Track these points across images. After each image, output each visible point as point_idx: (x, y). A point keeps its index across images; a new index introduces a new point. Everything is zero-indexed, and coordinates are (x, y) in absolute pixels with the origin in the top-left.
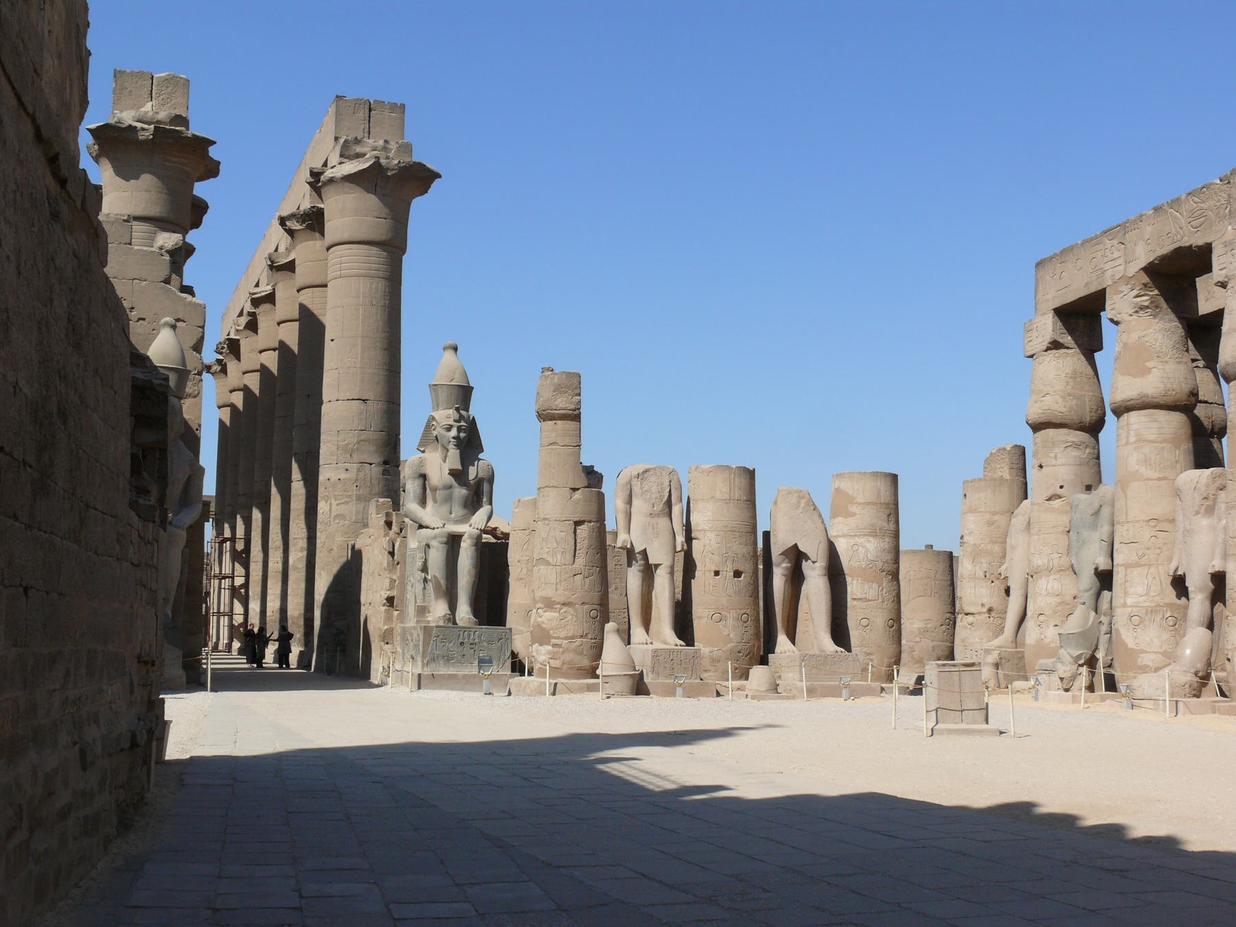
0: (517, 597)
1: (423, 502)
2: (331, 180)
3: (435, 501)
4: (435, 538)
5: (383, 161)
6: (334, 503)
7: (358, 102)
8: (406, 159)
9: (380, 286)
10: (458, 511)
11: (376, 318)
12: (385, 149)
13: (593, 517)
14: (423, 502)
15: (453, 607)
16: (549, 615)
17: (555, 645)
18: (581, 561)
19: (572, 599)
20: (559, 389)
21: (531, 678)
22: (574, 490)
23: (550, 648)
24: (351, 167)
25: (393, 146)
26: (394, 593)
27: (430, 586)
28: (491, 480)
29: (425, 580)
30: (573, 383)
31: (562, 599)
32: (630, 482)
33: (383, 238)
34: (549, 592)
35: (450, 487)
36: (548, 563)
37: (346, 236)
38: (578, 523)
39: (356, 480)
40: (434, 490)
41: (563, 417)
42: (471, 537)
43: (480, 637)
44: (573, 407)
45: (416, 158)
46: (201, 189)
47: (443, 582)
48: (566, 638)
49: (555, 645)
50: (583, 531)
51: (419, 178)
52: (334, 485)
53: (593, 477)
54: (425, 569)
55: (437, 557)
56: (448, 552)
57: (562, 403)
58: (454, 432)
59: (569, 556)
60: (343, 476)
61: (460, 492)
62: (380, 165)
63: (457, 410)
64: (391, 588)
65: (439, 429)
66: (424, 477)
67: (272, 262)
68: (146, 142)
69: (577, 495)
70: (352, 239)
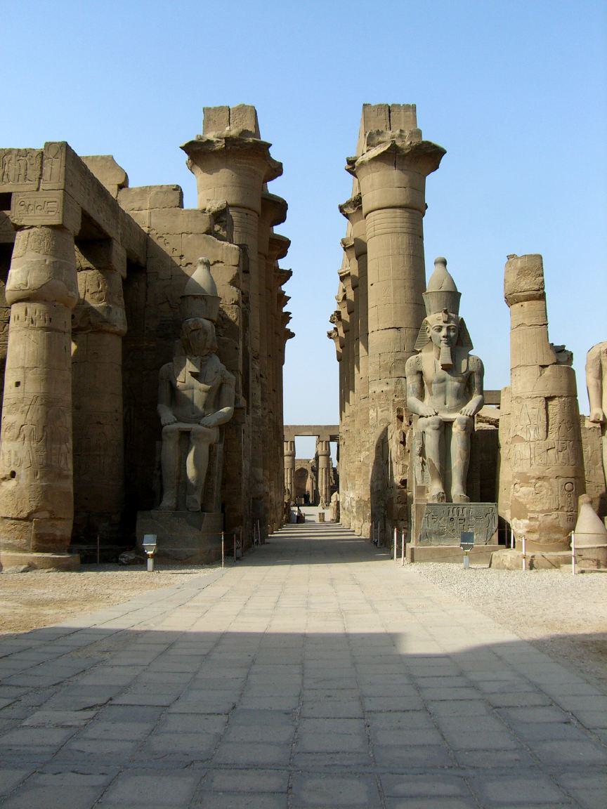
0: (506, 473)
1: (421, 396)
2: (362, 164)
3: (431, 394)
4: (428, 425)
5: (399, 144)
6: (379, 410)
7: (380, 107)
8: (416, 141)
9: (404, 239)
10: (451, 401)
11: (403, 263)
12: (401, 136)
13: (564, 393)
14: (421, 396)
15: (447, 486)
16: (524, 489)
17: (531, 519)
18: (553, 436)
19: (547, 473)
20: (522, 272)
21: (514, 550)
22: (543, 367)
23: (527, 521)
24: (376, 152)
25: (407, 134)
26: (406, 477)
27: (427, 468)
28: (481, 372)
29: (423, 463)
30: (534, 265)
31: (537, 474)
32: (599, 357)
33: (404, 203)
34: (524, 468)
35: (444, 380)
36: (522, 440)
37: (376, 205)
38: (548, 399)
39: (395, 391)
40: (430, 384)
41: (530, 298)
42: (460, 422)
43: (468, 512)
44: (537, 287)
45: (425, 138)
46: (274, 188)
47: (437, 465)
48: (541, 512)
49: (531, 519)
50: (555, 406)
51: (429, 156)
52: (379, 396)
53: (562, 356)
54: (422, 453)
55: (431, 442)
56: (440, 437)
57: (527, 284)
58: (444, 332)
59: (542, 432)
60: (385, 388)
61: (453, 383)
62: (396, 146)
63: (446, 312)
64: (404, 473)
65: (432, 331)
66: (420, 373)
67: (345, 245)
68: (221, 150)
69: (547, 371)
70: (381, 206)
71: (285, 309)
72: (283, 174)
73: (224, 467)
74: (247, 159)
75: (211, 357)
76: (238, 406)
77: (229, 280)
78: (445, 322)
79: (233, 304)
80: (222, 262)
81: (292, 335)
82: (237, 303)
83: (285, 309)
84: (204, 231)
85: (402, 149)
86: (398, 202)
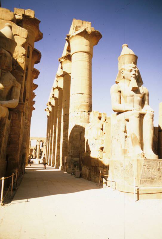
35: (133, 96)
71: (34, 100)
72: (43, 39)
73: (10, 135)
74: (30, 26)
75: (7, 72)
76: (20, 103)
77: (21, 44)
78: (133, 68)
79: (22, 55)
80: (18, 35)
81: (34, 109)
82: (24, 55)
83: (34, 100)
84: (11, 20)
85: (88, 32)
86: (85, 51)
